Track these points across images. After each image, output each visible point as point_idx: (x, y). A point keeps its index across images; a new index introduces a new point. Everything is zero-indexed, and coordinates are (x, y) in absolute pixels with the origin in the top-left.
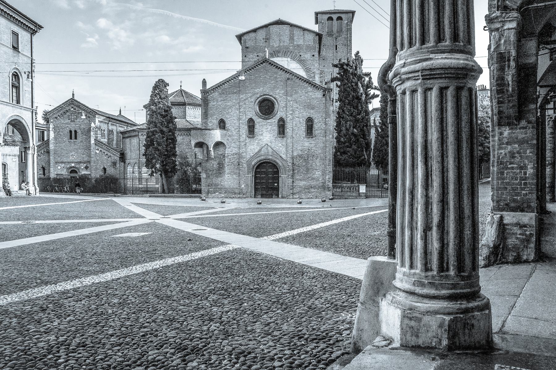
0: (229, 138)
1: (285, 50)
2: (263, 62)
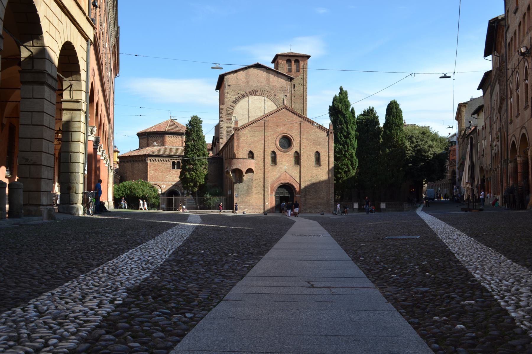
0: (256, 166)
1: (262, 89)
2: (283, 108)
